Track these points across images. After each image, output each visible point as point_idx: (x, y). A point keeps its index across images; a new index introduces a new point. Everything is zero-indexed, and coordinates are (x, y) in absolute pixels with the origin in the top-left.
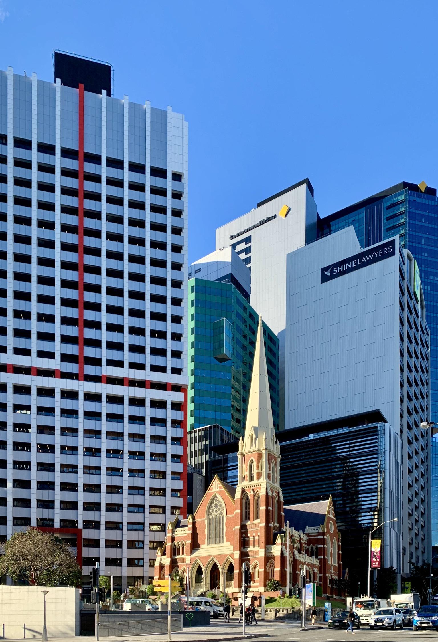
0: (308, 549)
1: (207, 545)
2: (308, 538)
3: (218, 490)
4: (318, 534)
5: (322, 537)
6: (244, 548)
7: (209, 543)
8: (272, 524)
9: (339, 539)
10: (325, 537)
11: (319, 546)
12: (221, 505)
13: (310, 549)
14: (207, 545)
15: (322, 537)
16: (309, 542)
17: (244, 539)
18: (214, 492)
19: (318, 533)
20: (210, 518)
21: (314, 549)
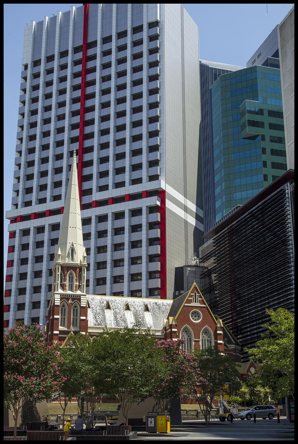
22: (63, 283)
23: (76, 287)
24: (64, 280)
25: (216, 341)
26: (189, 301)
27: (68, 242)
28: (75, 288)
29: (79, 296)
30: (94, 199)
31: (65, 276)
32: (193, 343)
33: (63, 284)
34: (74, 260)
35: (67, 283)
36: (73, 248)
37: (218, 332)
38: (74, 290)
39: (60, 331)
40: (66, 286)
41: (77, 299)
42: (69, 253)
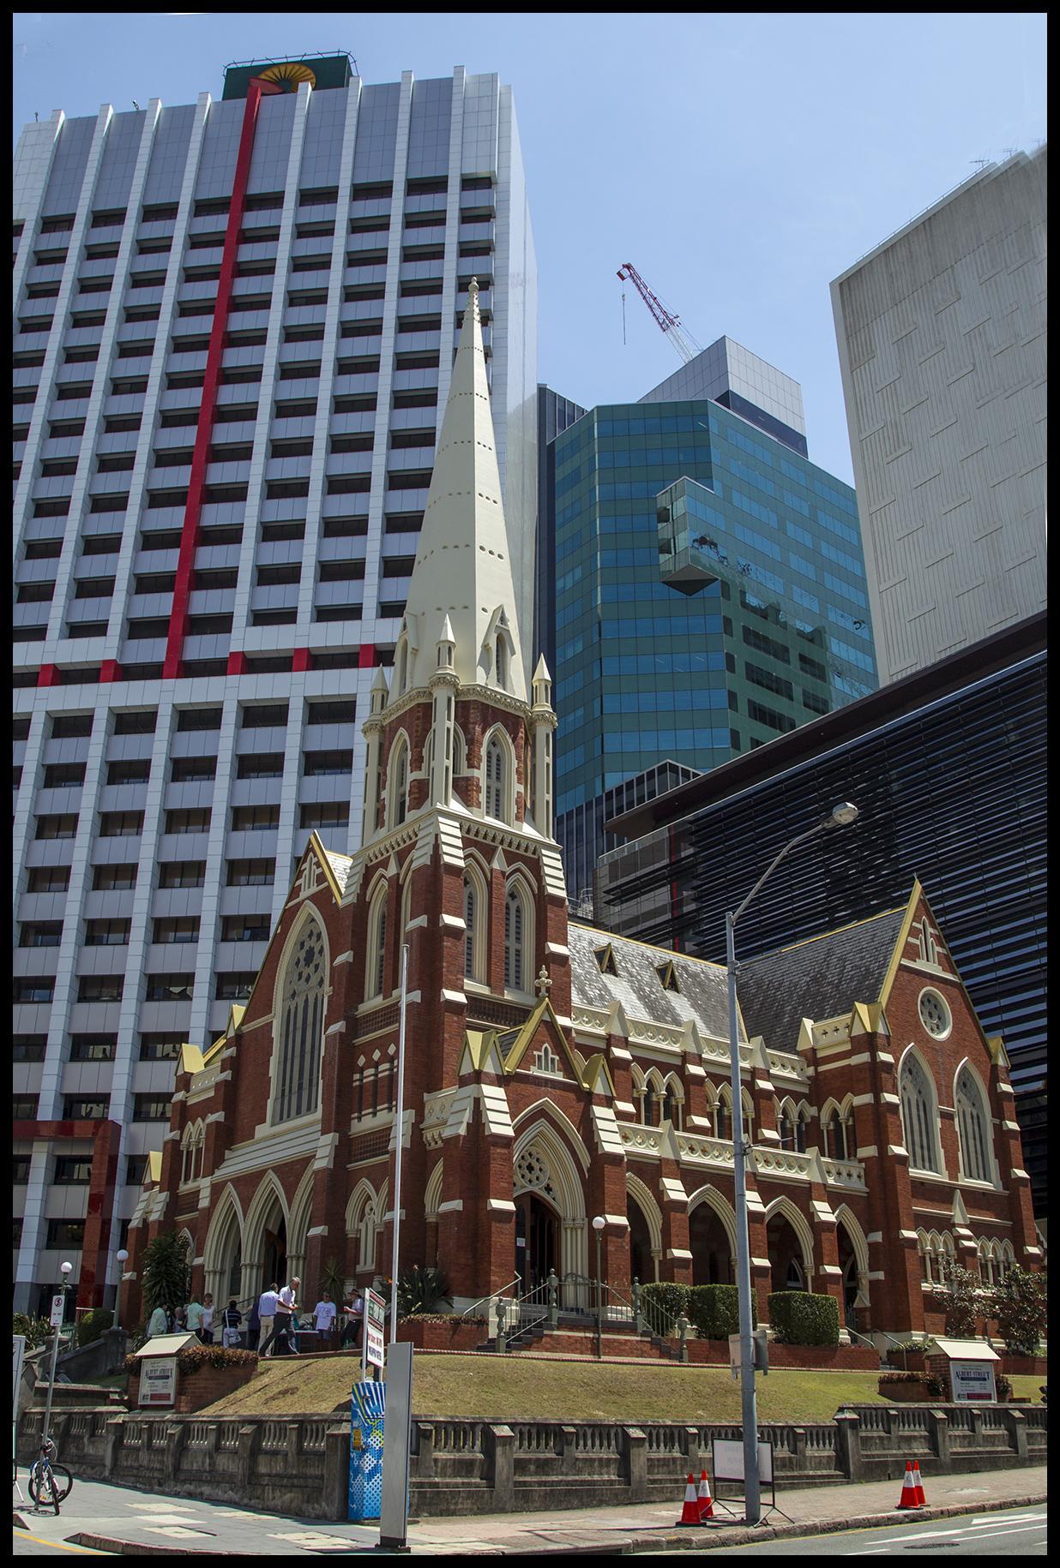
0: (816, 1120)
1: (273, 1125)
2: (811, 1071)
3: (314, 889)
4: (848, 1047)
5: (864, 1057)
6: (359, 1119)
7: (281, 1117)
8: (460, 989)
9: (995, 1067)
10: (885, 1057)
11: (859, 1100)
12: (321, 951)
13: (825, 1117)
14: (273, 1125)
15: (864, 1057)
16: (818, 1090)
17: (361, 1080)
18: (303, 901)
19: (852, 1039)
20: (289, 1011)
21: (843, 1114)
22: (465, 772)
23: (517, 803)
24: (469, 758)
25: (997, 1121)
26: (911, 952)
27: (479, 604)
28: (514, 809)
29: (532, 848)
30: (234, 649)
31: (472, 743)
32: (938, 1123)
33: (467, 779)
34: (508, 684)
35: (480, 774)
36: (504, 633)
37: (1006, 1088)
38: (513, 816)
39: (471, 997)
40: (479, 790)
41: (525, 860)
42: (486, 647)
